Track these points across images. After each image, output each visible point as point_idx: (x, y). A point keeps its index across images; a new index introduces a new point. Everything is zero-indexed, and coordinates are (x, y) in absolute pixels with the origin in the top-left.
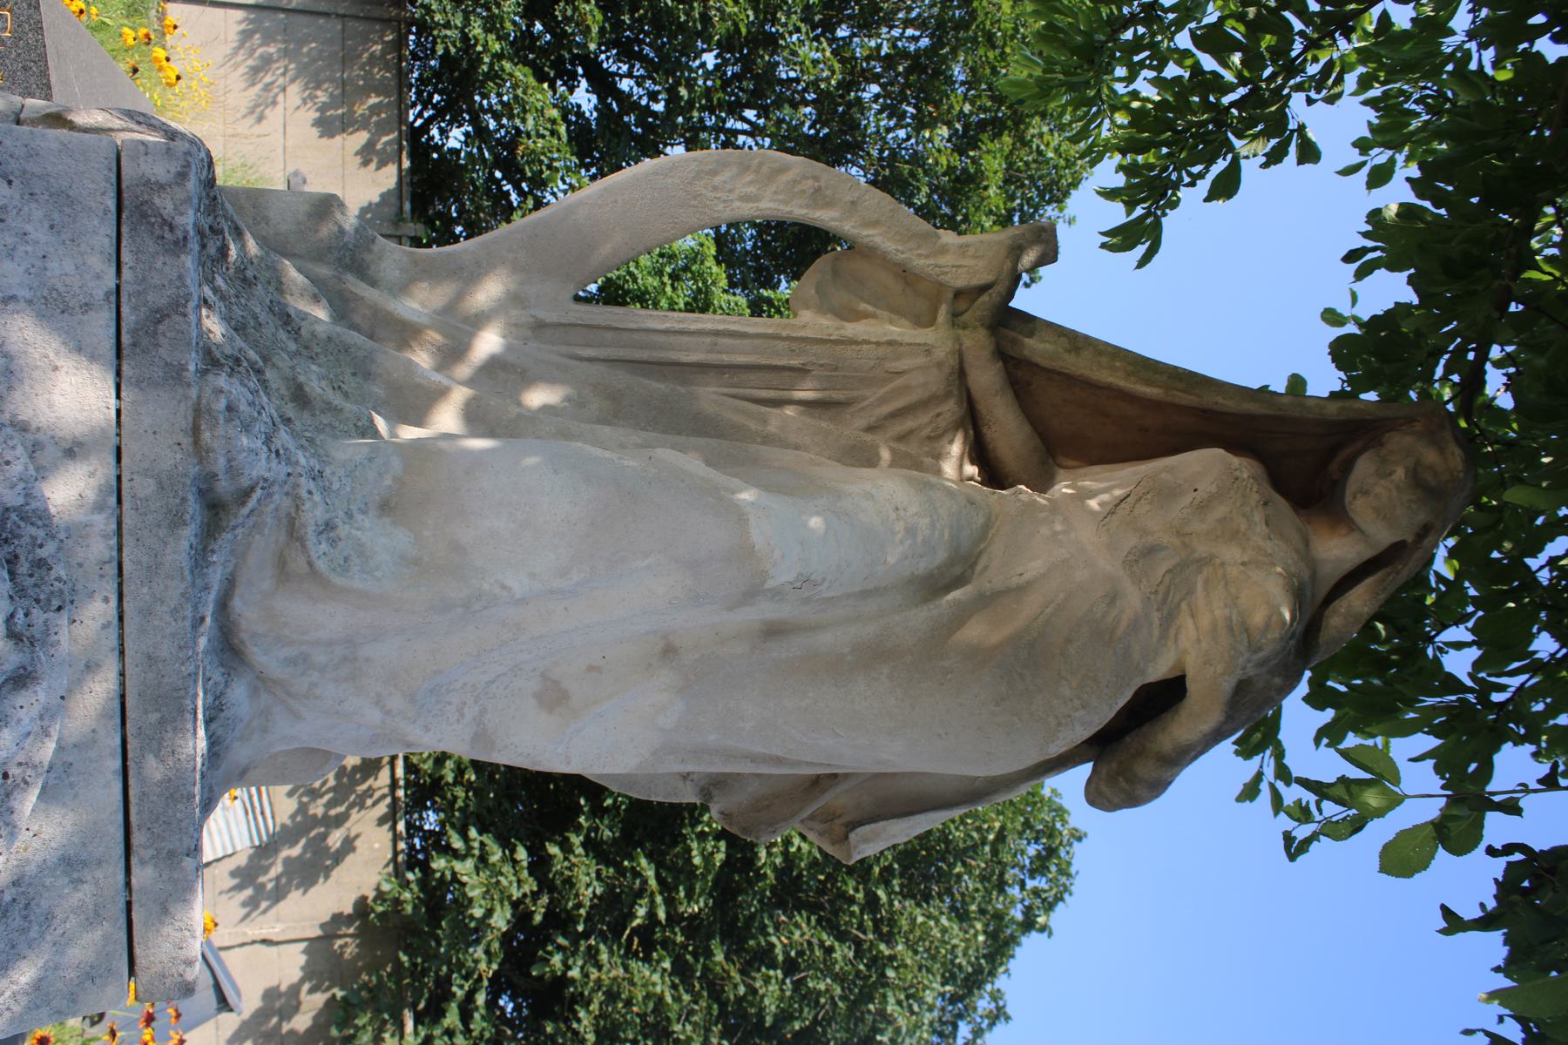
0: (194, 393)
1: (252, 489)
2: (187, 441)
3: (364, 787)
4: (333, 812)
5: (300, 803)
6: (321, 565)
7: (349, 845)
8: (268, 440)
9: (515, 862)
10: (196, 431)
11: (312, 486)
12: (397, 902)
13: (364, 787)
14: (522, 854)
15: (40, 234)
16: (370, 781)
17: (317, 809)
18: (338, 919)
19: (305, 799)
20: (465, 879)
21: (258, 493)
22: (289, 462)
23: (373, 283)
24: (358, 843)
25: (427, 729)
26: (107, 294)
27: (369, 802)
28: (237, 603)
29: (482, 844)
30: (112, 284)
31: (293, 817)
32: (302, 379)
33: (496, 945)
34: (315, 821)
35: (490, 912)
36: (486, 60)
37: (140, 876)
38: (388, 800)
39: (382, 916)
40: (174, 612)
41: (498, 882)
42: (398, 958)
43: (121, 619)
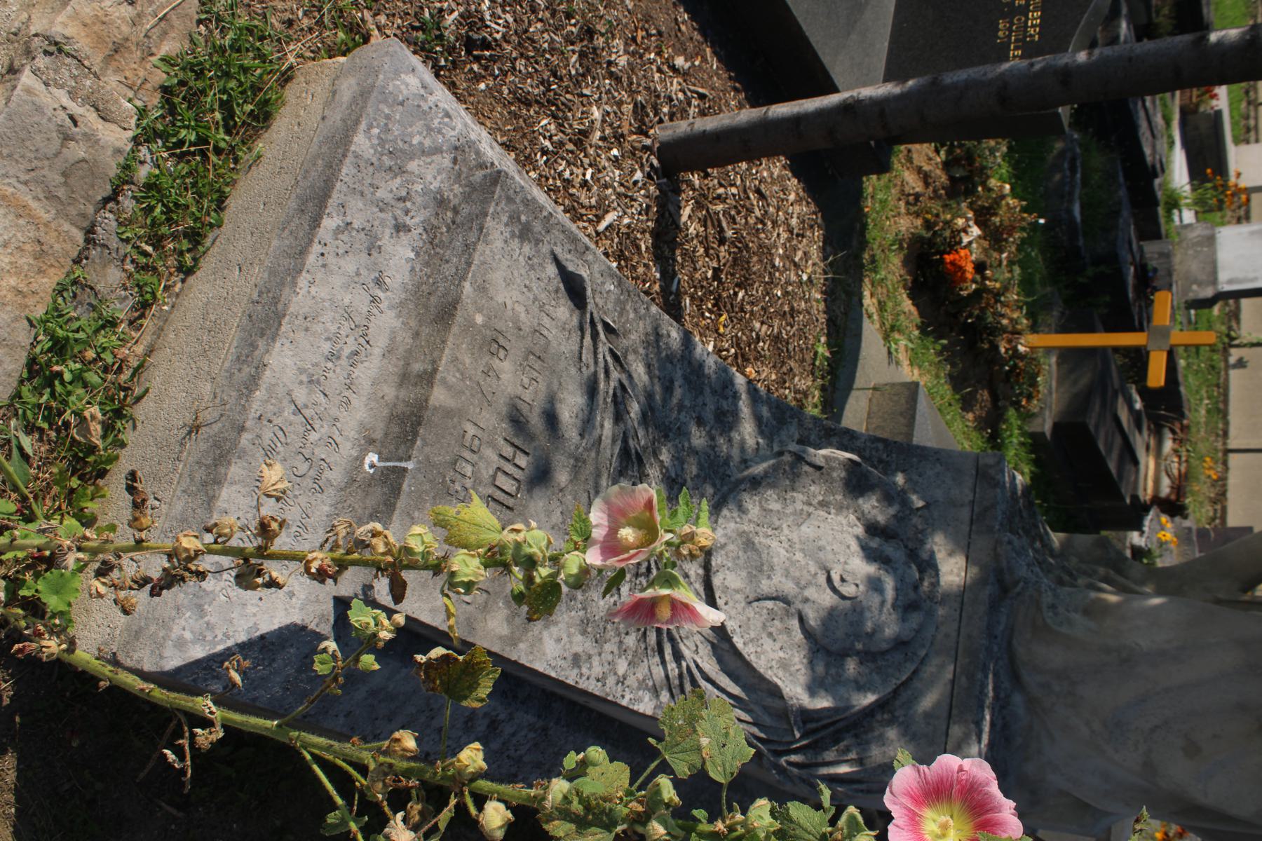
6: (1049, 621)
8: (1028, 565)
10: (995, 549)
21: (1021, 584)
23: (1127, 578)
28: (1015, 642)
30: (971, 497)
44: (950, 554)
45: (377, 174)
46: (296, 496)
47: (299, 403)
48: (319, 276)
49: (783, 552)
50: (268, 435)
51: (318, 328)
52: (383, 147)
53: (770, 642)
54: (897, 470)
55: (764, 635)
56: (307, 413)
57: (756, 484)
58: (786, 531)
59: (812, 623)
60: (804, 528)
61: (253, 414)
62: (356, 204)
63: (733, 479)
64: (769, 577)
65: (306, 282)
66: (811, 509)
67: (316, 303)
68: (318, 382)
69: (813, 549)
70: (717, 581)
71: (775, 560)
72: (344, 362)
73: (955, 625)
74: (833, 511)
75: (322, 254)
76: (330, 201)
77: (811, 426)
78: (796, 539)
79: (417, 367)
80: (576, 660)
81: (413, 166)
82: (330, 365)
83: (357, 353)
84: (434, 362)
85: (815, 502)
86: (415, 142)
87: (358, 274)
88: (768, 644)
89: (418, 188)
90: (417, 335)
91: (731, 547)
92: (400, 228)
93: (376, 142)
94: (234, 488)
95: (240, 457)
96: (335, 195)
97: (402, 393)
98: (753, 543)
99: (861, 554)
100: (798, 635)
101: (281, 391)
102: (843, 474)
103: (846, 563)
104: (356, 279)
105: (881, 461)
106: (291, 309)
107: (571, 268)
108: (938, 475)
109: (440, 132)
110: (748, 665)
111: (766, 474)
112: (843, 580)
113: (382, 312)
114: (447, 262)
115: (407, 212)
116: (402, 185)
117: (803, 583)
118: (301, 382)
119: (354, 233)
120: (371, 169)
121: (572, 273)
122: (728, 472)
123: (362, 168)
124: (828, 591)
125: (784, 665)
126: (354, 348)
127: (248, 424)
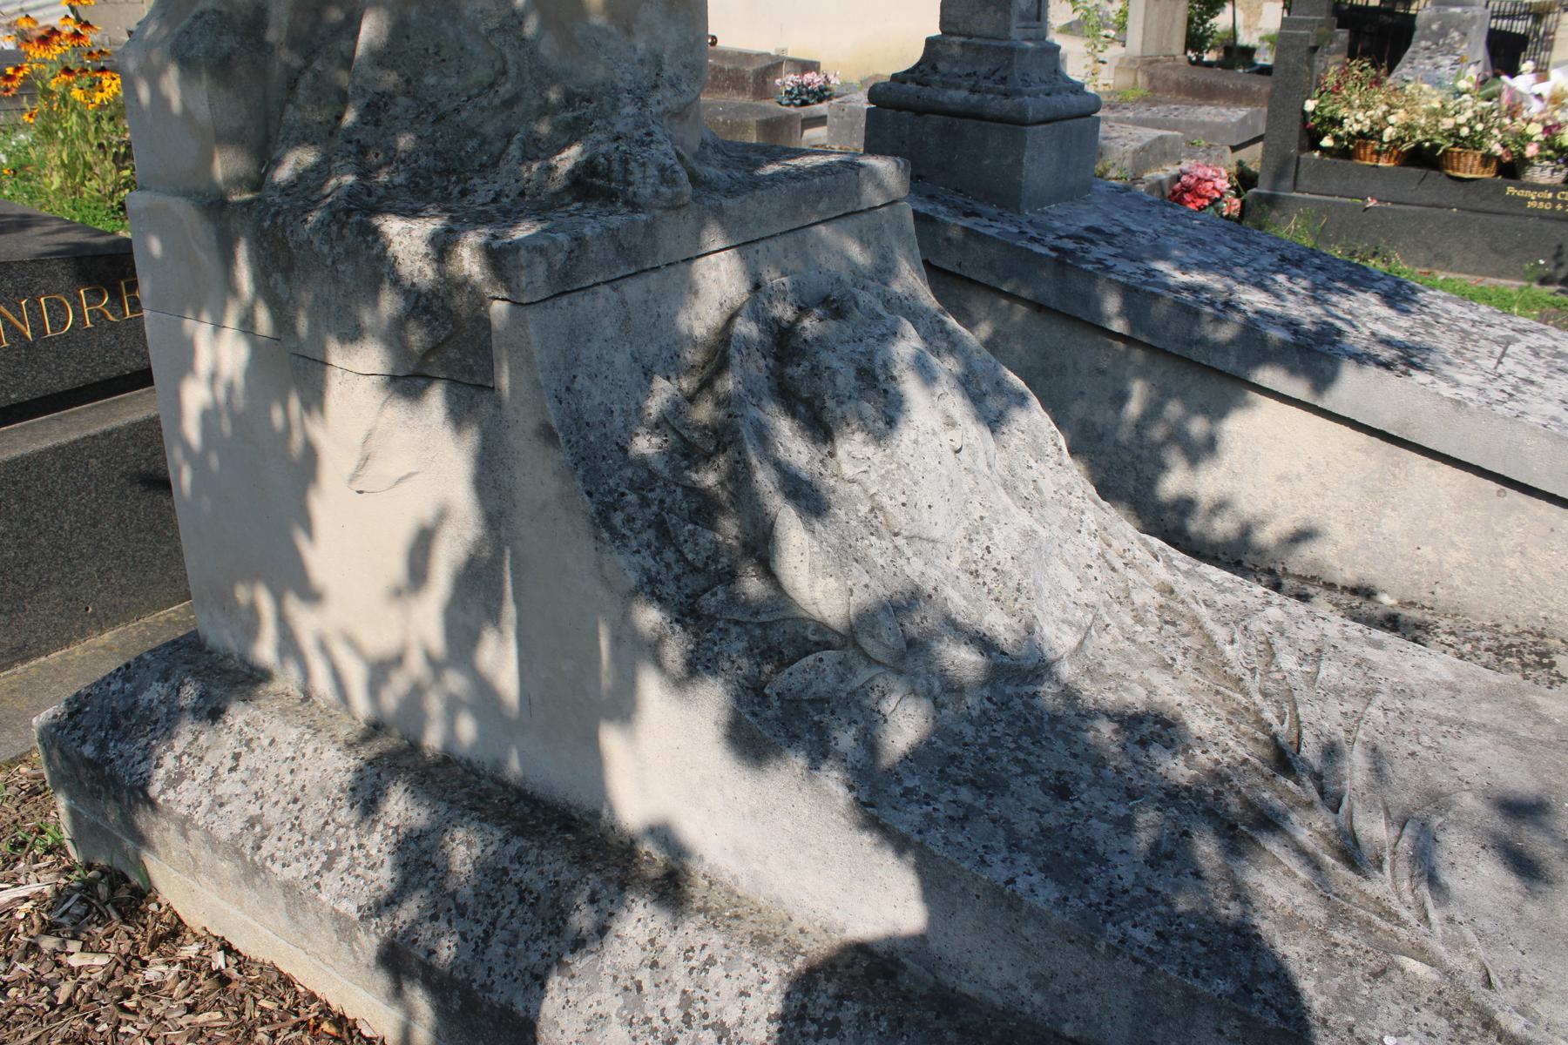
0: (658, 212)
8: (641, 143)
11: (651, 101)
15: (595, 345)
22: (645, 125)
26: (615, 289)
30: (605, 290)
32: (497, 101)
40: (760, 203)
43: (758, 241)
44: (696, 293)
53: (1041, 483)
54: (631, 463)
55: (1048, 496)
57: (984, 644)
60: (936, 533)
63: (986, 693)
71: (1016, 536)
73: (771, 243)
74: (864, 509)
77: (727, 665)
78: (959, 533)
80: (1378, 645)
88: (1047, 486)
99: (902, 419)
102: (818, 526)
103: (934, 433)
105: (645, 503)
108: (593, 377)
111: (957, 641)
122: (988, 705)
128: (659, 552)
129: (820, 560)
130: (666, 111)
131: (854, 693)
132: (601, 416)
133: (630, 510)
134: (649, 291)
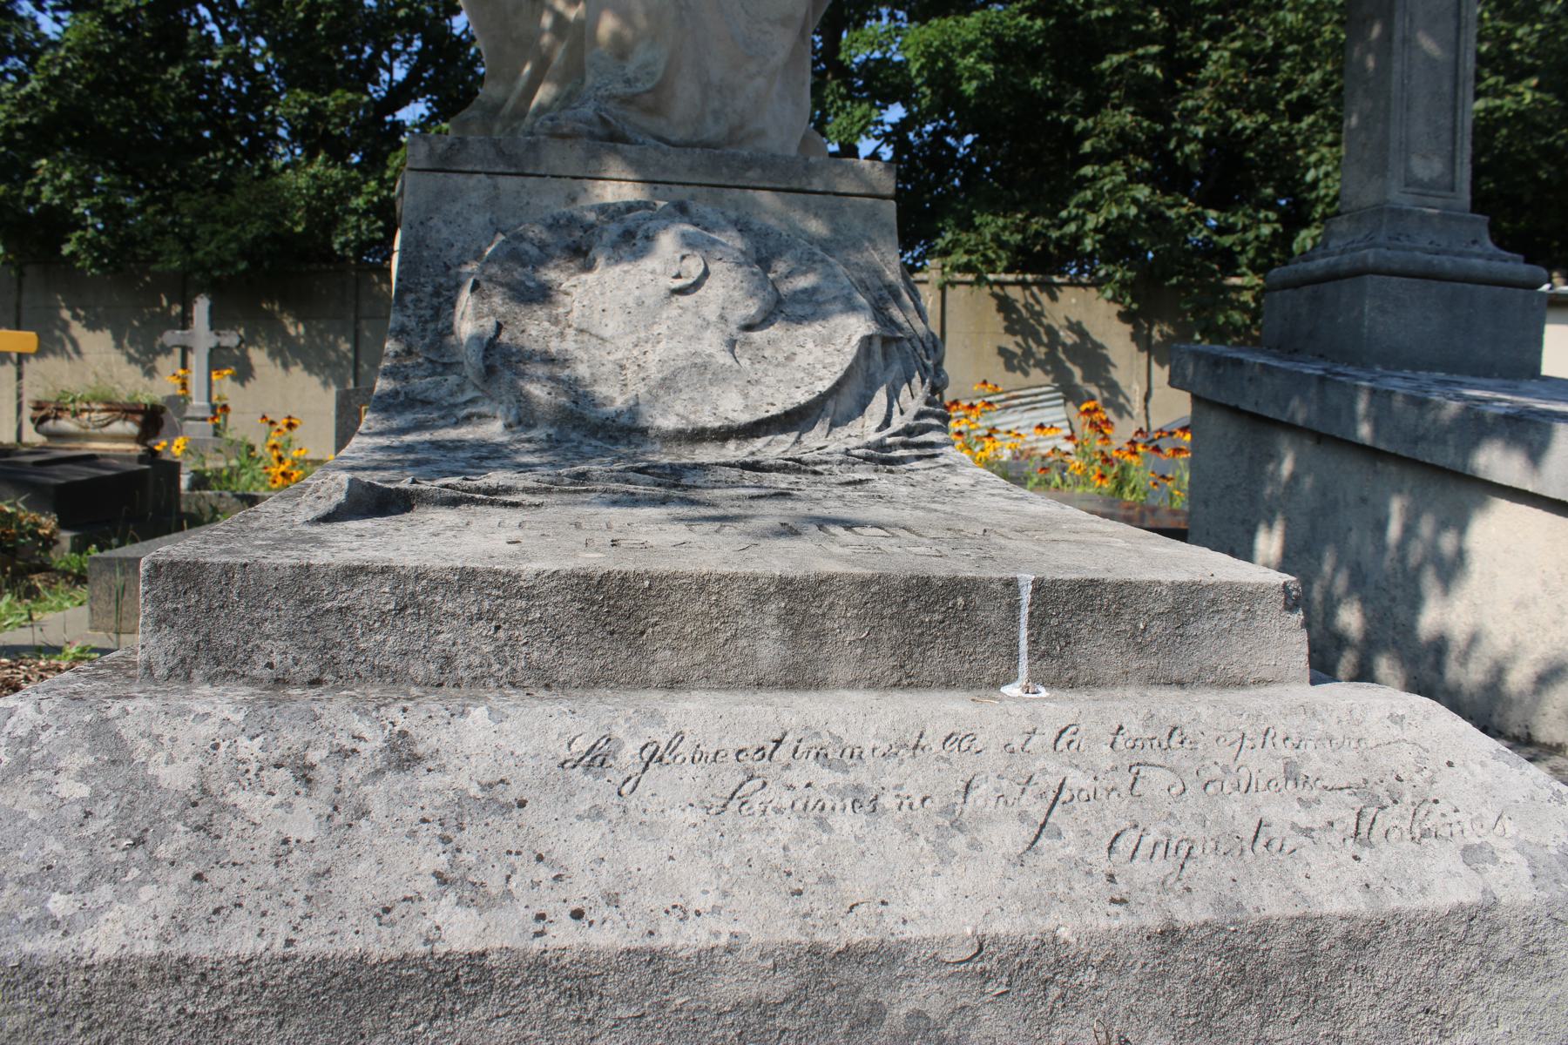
1: (601, 117)
2: (569, 142)
3: (1024, 311)
4: (1045, 339)
5: (1035, 366)
6: (649, 86)
7: (1077, 328)
9: (1094, 178)
12: (1123, 284)
13: (1024, 311)
14: (1087, 170)
15: (457, 207)
16: (1019, 306)
17: (1041, 352)
18: (1135, 337)
19: (1032, 362)
20: (1101, 219)
24: (1074, 320)
25: (774, 53)
27: (1037, 308)
28: (673, 139)
29: (1078, 206)
30: (482, 176)
31: (1047, 373)
33: (1168, 199)
34: (1051, 354)
35: (1135, 201)
36: (385, 193)
37: (817, 184)
38: (1035, 289)
39: (1134, 300)
41: (1109, 191)
42: (1173, 286)
45: (234, 854)
46: (1226, 770)
47: (1028, 833)
48: (651, 901)
49: (662, 345)
50: (1146, 871)
51: (806, 856)
52: (125, 866)
56: (1038, 811)
58: (619, 355)
59: (753, 311)
60: (607, 333)
61: (1123, 920)
62: (362, 881)
63: (551, 431)
64: (710, 355)
65: (689, 928)
66: (568, 331)
67: (737, 882)
68: (947, 810)
69: (641, 313)
70: (745, 418)
72: (860, 775)
73: (675, 188)
75: (577, 915)
76: (376, 952)
78: (634, 338)
79: (769, 651)
81: (176, 776)
82: (888, 801)
83: (821, 756)
84: (759, 598)
85: (557, 330)
86: (84, 791)
87: (597, 813)
88: (803, 359)
89: (249, 748)
90: (673, 684)
91: (679, 408)
92: (403, 755)
93: (105, 891)
94: (1309, 890)
95: (1239, 907)
96: (351, 945)
97: (842, 671)
98: (664, 379)
100: (774, 331)
101: (1026, 882)
104: (614, 813)
106: (792, 935)
107: (340, 497)
108: (447, 223)
109: (31, 739)
110: (848, 374)
112: (678, 276)
113: (680, 736)
114: (448, 661)
115: (346, 754)
116: (256, 784)
117: (699, 322)
118: (974, 845)
119: (468, 858)
120: (217, 877)
121: (349, 494)
123: (221, 899)
124: (700, 292)
125: (825, 341)
126: (812, 765)
127: (1153, 921)
128: (426, 322)
129: (469, 311)
130: (612, 97)
131: (455, 406)
132: (442, 246)
133: (421, 295)
134: (524, 186)
